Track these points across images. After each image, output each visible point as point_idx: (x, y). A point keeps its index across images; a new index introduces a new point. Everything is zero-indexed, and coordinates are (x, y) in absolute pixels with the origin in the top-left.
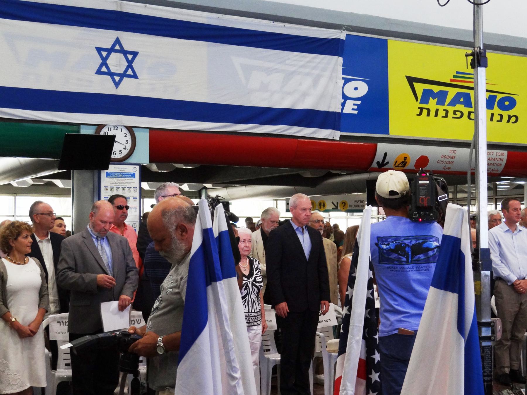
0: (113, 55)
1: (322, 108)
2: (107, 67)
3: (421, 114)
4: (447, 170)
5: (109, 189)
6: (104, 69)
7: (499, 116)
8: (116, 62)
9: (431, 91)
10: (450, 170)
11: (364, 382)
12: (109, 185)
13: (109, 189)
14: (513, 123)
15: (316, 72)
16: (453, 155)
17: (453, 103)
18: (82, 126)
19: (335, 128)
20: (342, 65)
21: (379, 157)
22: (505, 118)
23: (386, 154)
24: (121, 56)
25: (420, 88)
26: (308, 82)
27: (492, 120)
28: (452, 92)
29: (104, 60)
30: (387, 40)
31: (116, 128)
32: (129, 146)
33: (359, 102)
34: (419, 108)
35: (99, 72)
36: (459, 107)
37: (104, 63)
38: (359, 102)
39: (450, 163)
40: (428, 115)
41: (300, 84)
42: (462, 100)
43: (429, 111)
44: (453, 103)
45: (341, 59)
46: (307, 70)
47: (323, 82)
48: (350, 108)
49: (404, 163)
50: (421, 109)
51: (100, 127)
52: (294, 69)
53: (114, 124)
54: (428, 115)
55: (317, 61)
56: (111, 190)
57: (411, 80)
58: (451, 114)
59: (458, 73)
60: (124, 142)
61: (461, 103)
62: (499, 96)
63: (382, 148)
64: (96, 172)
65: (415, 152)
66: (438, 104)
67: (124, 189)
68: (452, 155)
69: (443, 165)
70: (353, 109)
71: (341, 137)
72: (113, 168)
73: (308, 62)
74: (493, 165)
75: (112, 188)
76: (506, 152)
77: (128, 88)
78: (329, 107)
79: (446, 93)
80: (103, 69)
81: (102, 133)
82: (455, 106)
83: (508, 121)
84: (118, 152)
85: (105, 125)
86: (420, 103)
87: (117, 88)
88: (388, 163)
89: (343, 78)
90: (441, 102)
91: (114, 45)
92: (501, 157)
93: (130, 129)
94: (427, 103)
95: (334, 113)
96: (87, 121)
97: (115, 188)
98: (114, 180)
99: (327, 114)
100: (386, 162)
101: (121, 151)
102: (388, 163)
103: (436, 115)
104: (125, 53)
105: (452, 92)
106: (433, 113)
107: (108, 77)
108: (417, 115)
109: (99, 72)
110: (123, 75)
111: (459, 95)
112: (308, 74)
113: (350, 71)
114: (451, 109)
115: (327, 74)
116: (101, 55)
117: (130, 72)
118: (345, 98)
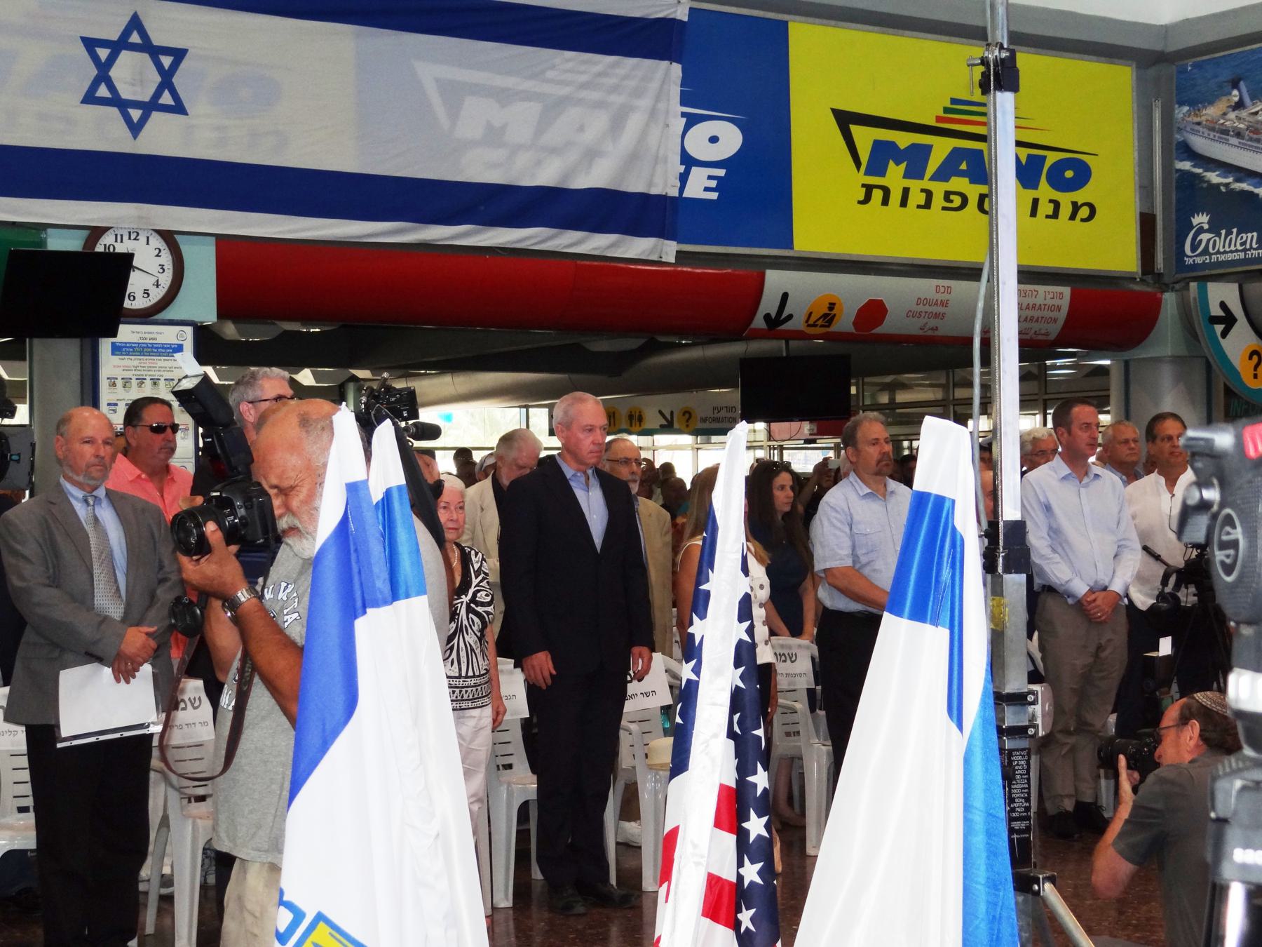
0: (125, 56)
1: (635, 185)
2: (111, 87)
3: (867, 199)
4: (930, 333)
5: (119, 383)
6: (103, 91)
8: (135, 76)
9: (892, 145)
11: (730, 840)
12: (119, 374)
13: (119, 383)
14: (1083, 220)
15: (617, 99)
16: (945, 297)
17: (943, 174)
18: (50, 231)
20: (679, 82)
21: (769, 304)
22: (1066, 210)
24: (145, 58)
25: (865, 137)
26: (599, 123)
27: (1034, 213)
28: (941, 148)
29: (103, 69)
30: (786, 23)
31: (134, 235)
32: (166, 279)
33: (721, 172)
34: (863, 185)
35: (90, 98)
36: (959, 184)
37: (103, 75)
38: (721, 172)
39: (937, 316)
40: (885, 202)
41: (581, 129)
42: (964, 166)
43: (886, 191)
44: (943, 174)
45: (676, 70)
46: (595, 95)
47: (635, 123)
48: (699, 186)
49: (828, 318)
50: (869, 189)
51: (96, 232)
52: (566, 91)
53: (130, 227)
54: (885, 202)
55: (621, 71)
56: (124, 386)
57: (845, 119)
58: (938, 201)
59: (954, 101)
60: (154, 269)
61: (962, 174)
62: (1052, 158)
63: (776, 280)
64: (88, 341)
65: (853, 291)
66: (907, 175)
67: (155, 382)
68: (940, 297)
69: (922, 321)
70: (707, 189)
72: (127, 333)
73: (600, 75)
75: (126, 382)
76: (1066, 291)
77: (164, 138)
78: (650, 184)
79: (927, 149)
80: (99, 92)
81: (99, 248)
82: (947, 180)
83: (1073, 217)
84: (139, 294)
85: (106, 229)
86: (867, 173)
87: (135, 138)
88: (790, 317)
89: (683, 114)
90: (915, 171)
91: (126, 33)
92: (1056, 302)
93: (169, 237)
94: (882, 173)
95: (663, 198)
96: (62, 220)
97: (134, 382)
98: (133, 361)
99: (645, 200)
101: (146, 292)
102: (790, 317)
103: (904, 203)
104: (154, 52)
105: (941, 148)
106: (896, 197)
107: (114, 111)
108: (860, 202)
109: (90, 98)
110: (150, 107)
111: (956, 154)
112: (600, 105)
113: (701, 97)
114: (938, 189)
115: (645, 103)
116: (95, 58)
117: (166, 99)
118: (688, 161)
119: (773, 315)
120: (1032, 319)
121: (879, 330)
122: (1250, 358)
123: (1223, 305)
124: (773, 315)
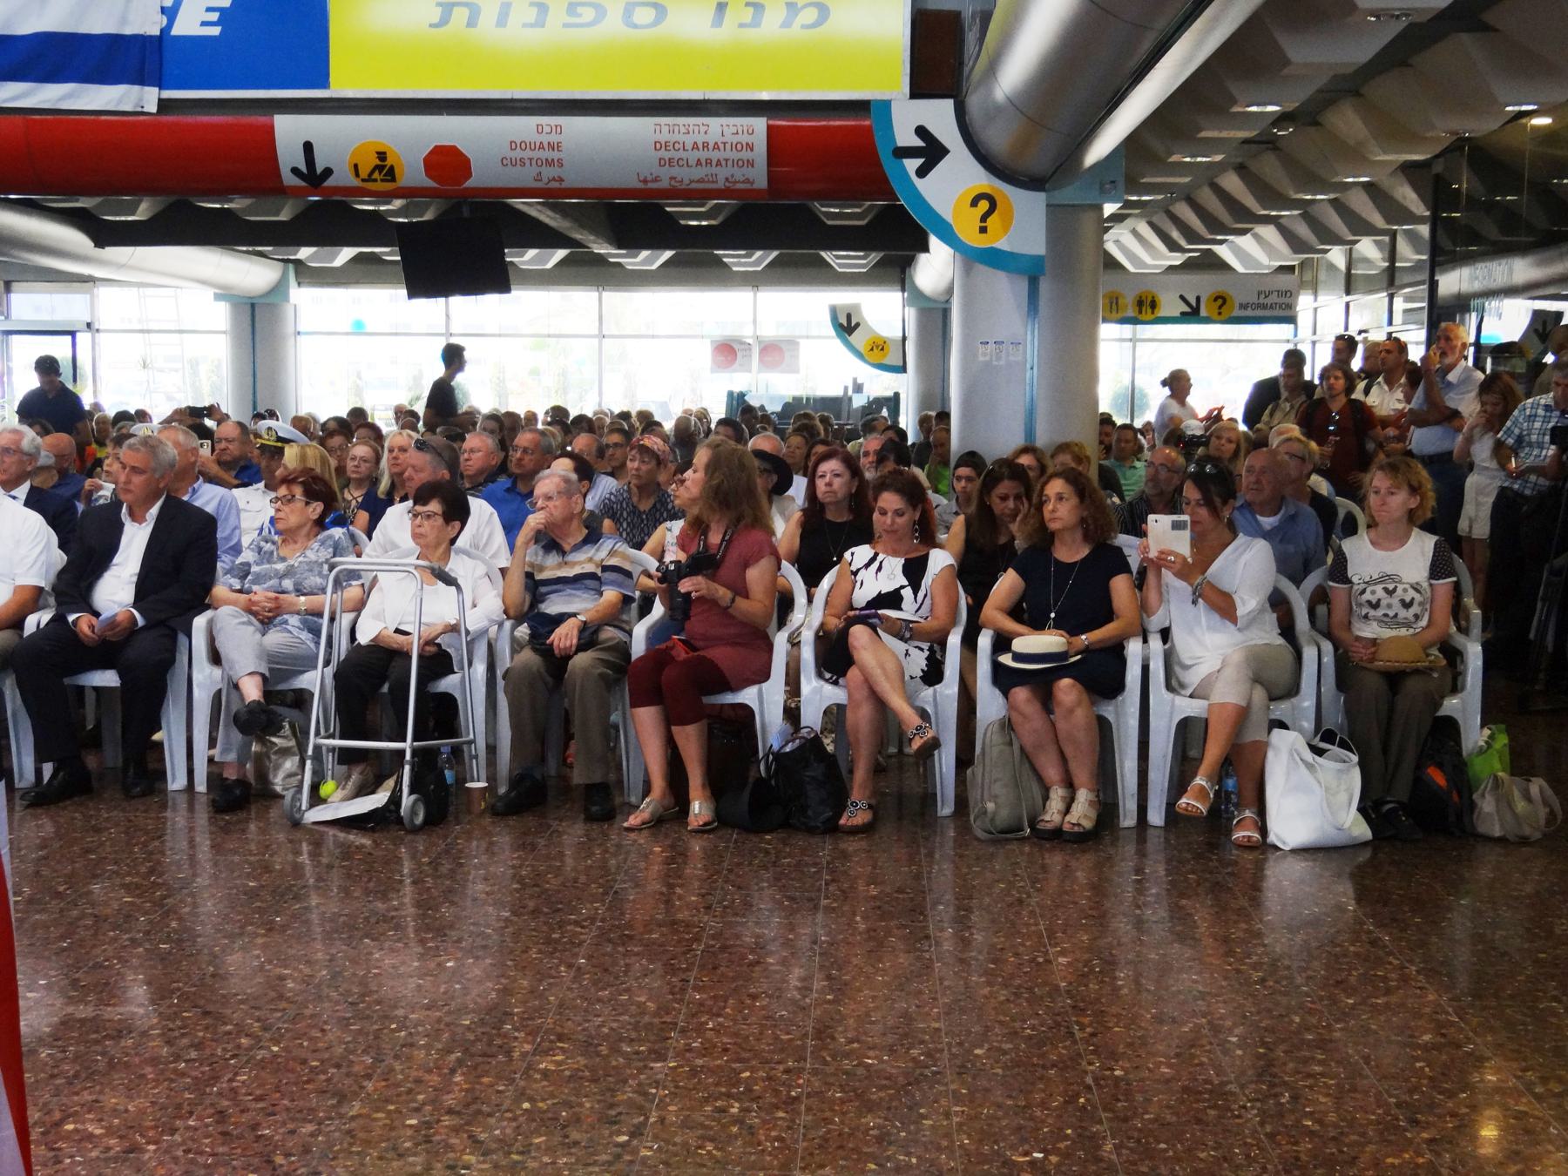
4: (555, 185)
7: (751, 10)
10: (564, 185)
16: (554, 138)
19: (141, 80)
21: (289, 155)
23: (308, 147)
34: (439, 4)
63: (290, 131)
65: (411, 138)
68: (545, 139)
70: (204, 24)
71: (164, 105)
74: (719, 163)
78: (124, 21)
92: (745, 139)
100: (319, 170)
102: (328, 172)
119: (304, 169)
120: (709, 162)
121: (470, 183)
122: (974, 203)
123: (921, 131)
124: (304, 169)
